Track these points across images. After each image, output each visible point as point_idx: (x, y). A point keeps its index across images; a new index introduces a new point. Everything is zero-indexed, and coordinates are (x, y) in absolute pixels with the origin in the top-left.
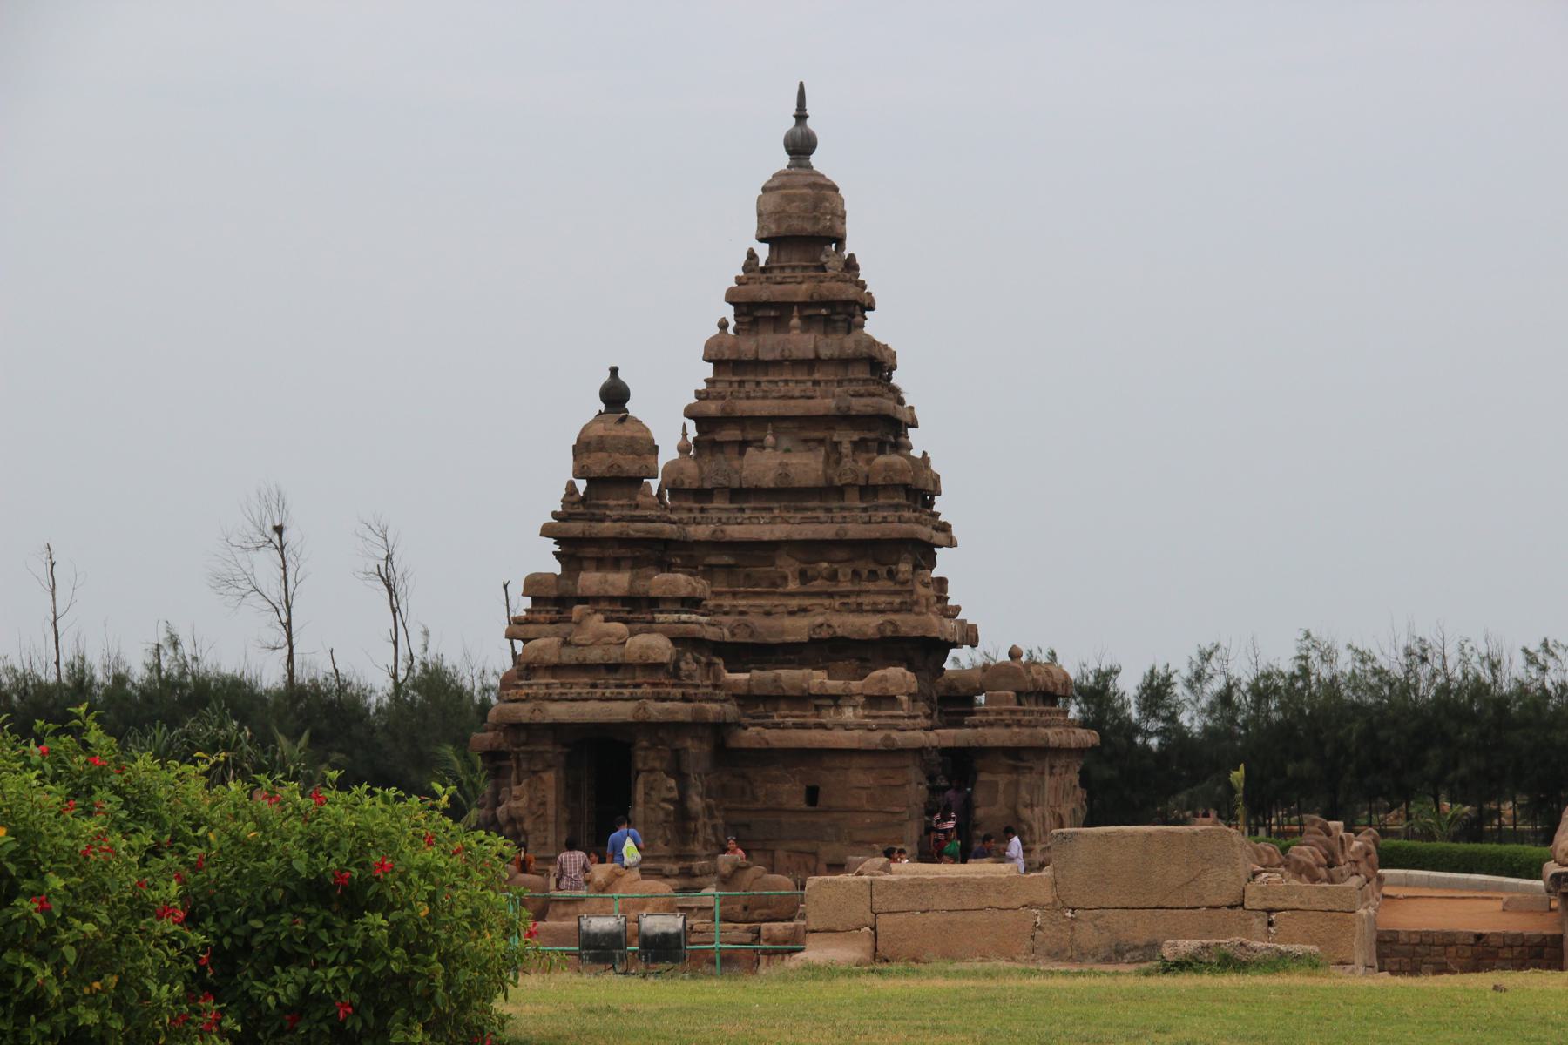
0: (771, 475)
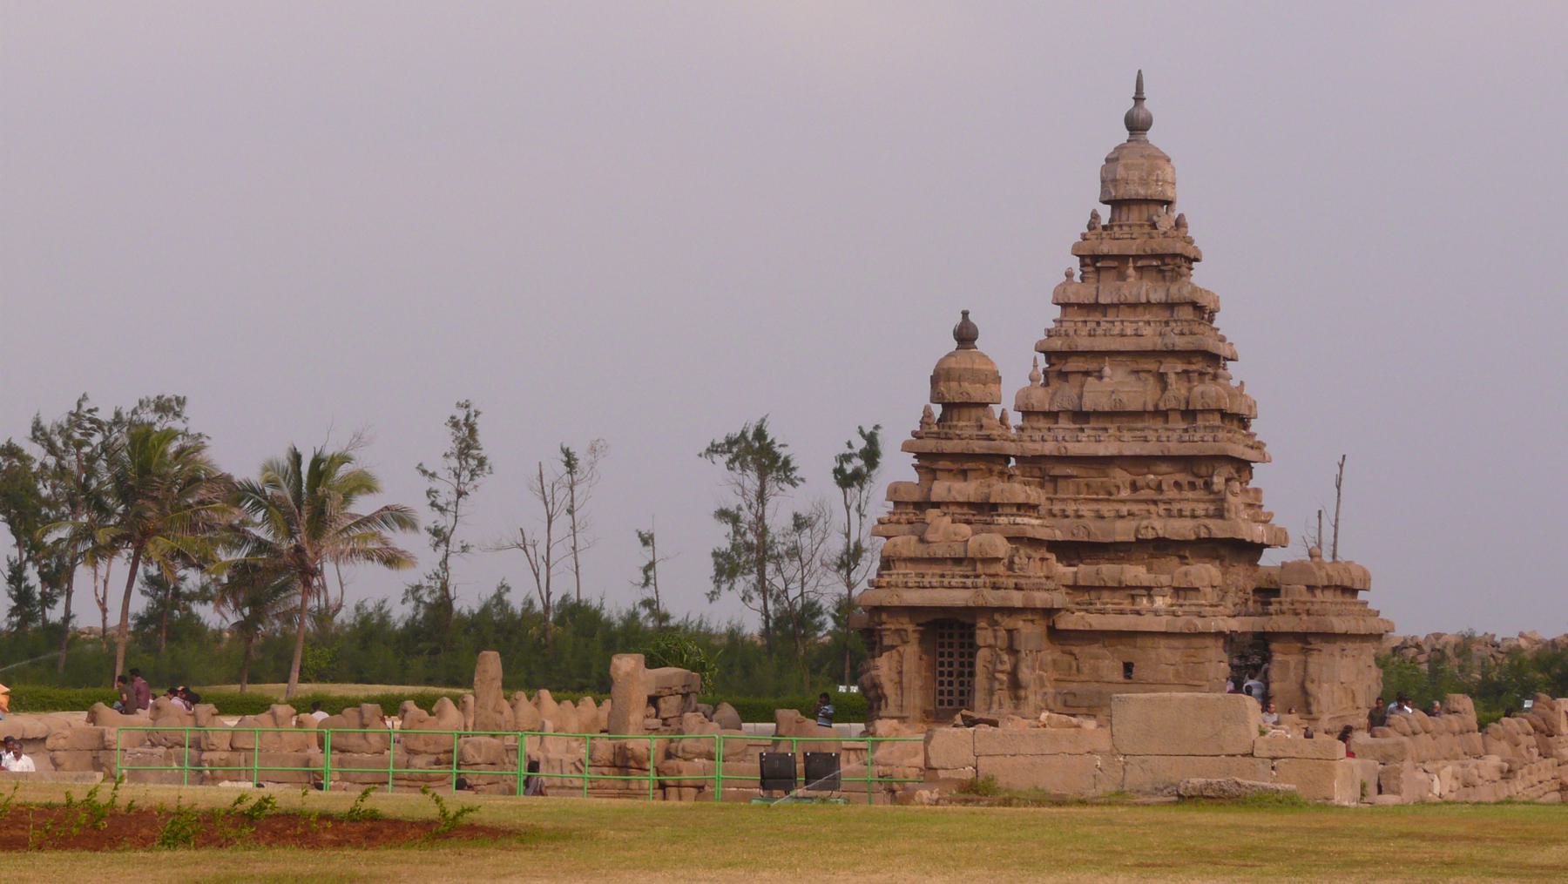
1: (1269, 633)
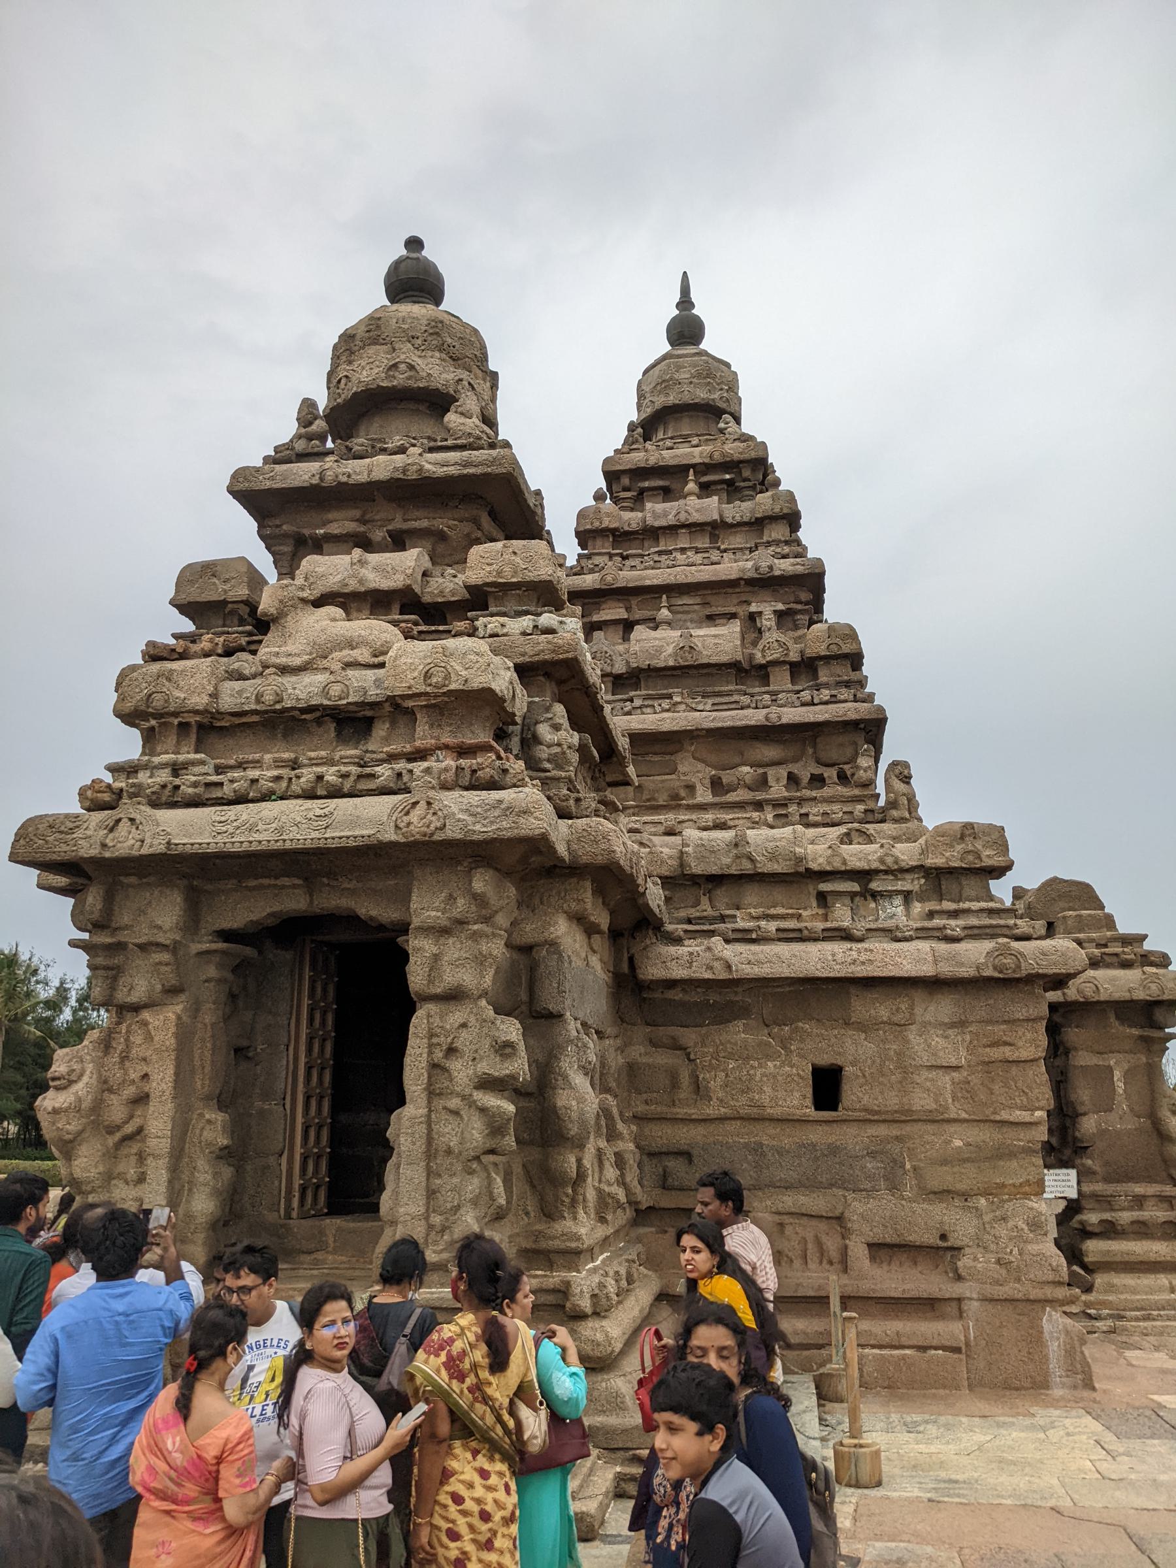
0: (670, 650)
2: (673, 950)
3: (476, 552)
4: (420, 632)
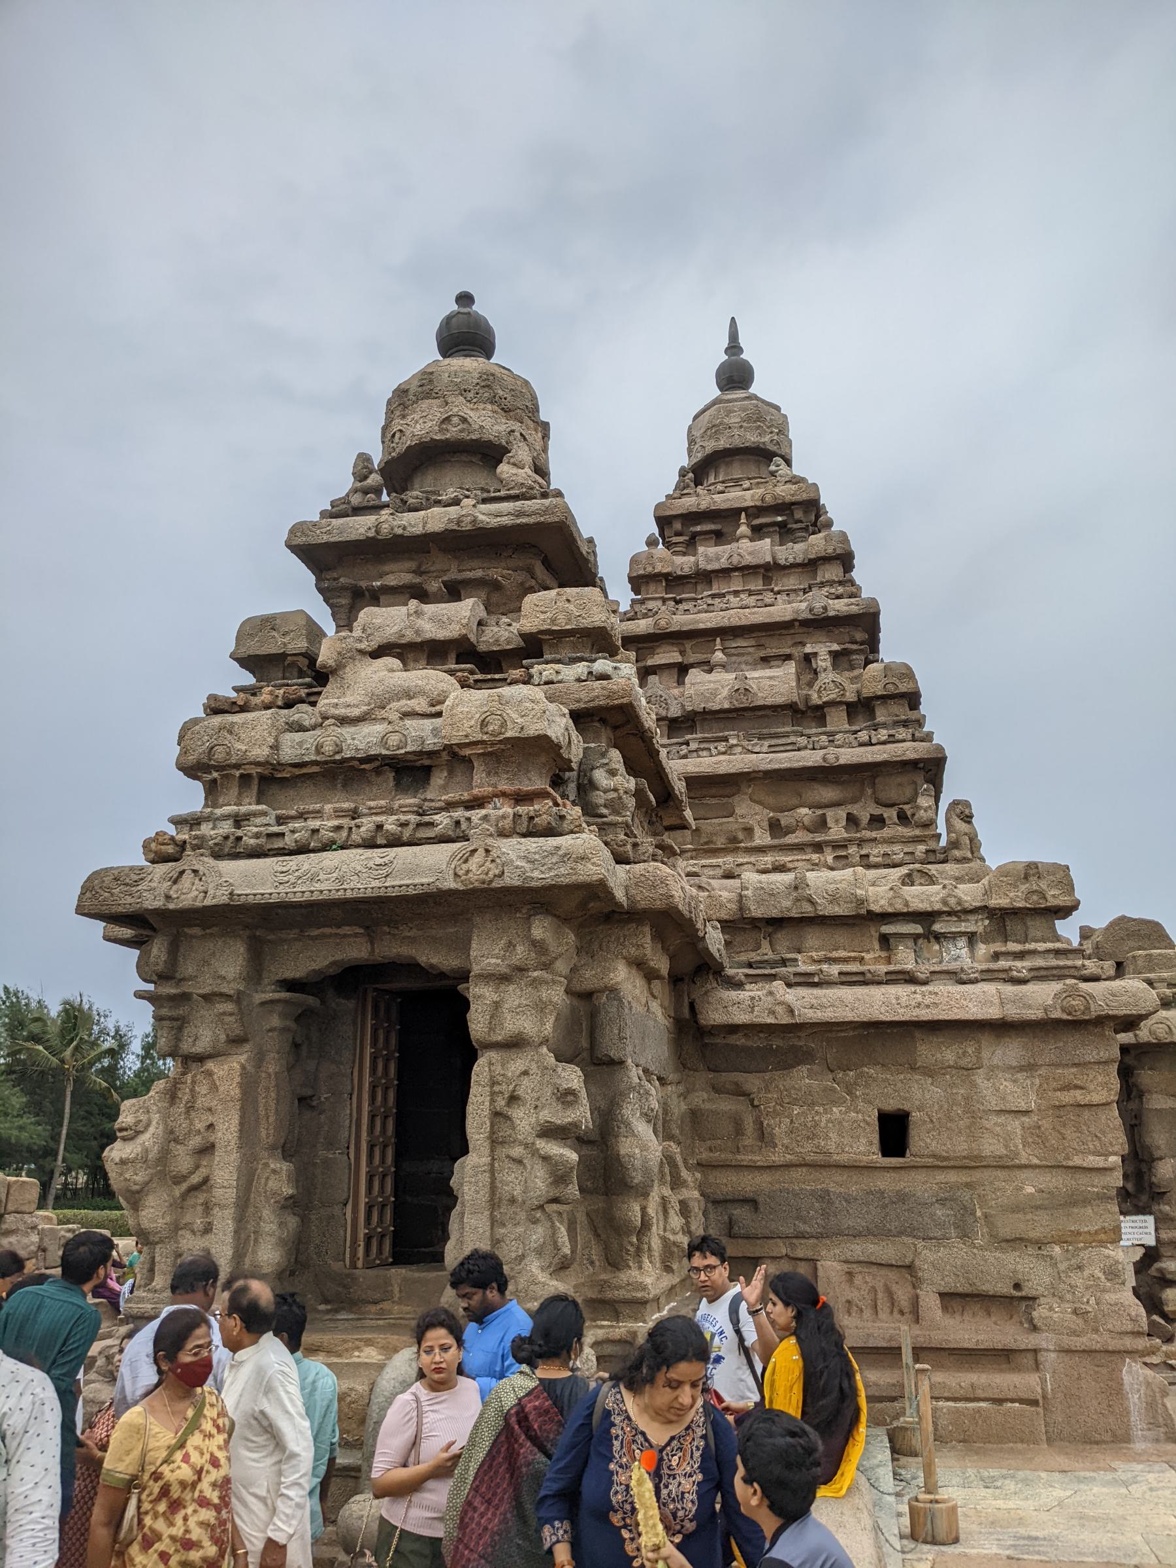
0: (725, 692)
1: (1149, 1044)
2: (733, 994)
3: (530, 600)
4: (476, 681)
